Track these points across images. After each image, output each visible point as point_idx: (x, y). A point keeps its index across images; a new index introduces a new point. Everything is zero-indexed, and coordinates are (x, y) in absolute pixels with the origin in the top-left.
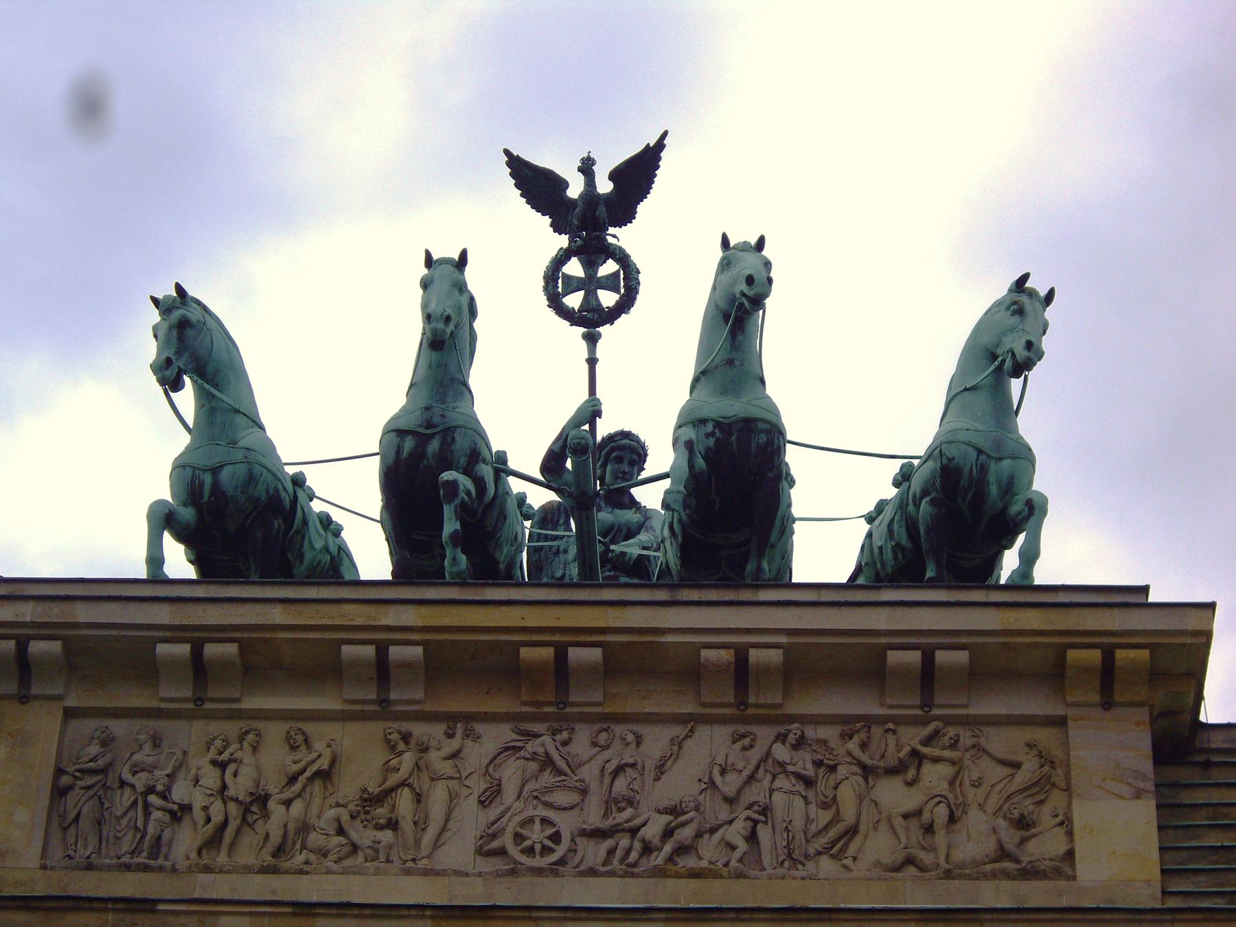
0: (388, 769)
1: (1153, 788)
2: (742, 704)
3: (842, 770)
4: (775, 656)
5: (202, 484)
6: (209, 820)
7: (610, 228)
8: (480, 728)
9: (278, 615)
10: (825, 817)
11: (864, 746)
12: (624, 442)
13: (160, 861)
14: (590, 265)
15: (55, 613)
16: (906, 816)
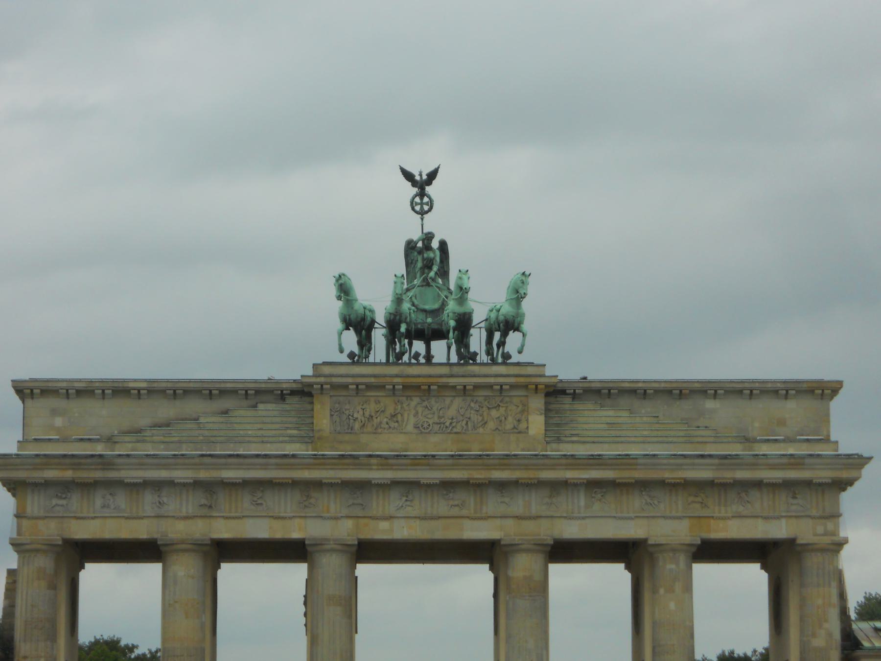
0: (395, 409)
1: (544, 412)
2: (465, 393)
3: (484, 409)
4: (471, 387)
5: (346, 318)
6: (362, 422)
7: (426, 187)
8: (413, 398)
9: (373, 380)
10: (480, 418)
11: (488, 402)
12: (429, 235)
13: (352, 432)
14: (422, 199)
15: (328, 380)
16: (496, 418)
